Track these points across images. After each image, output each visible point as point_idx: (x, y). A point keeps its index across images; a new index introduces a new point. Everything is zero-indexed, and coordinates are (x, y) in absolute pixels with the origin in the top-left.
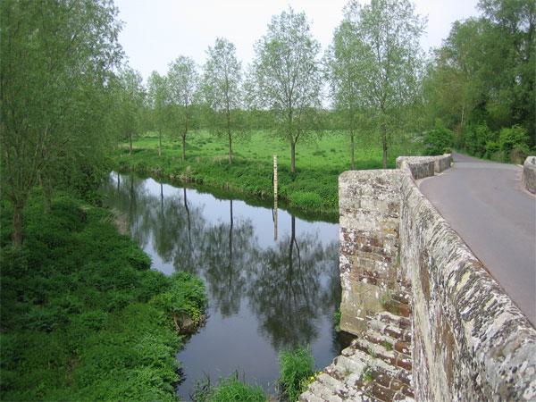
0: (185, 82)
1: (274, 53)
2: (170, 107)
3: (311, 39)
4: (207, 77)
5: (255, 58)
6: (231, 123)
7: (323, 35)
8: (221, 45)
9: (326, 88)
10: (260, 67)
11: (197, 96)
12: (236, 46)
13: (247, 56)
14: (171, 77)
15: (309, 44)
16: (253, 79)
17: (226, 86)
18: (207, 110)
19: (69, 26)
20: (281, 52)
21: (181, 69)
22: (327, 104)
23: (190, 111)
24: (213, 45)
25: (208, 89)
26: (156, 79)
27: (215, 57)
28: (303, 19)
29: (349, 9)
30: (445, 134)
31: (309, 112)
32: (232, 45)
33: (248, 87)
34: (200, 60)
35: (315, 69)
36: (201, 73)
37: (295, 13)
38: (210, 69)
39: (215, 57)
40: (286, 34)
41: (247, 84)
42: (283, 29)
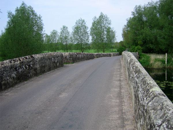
0: (55, 37)
1: (77, 30)
2: (51, 43)
3: (86, 26)
4: (61, 36)
5: (75, 25)
6: (67, 48)
7: (89, 25)
8: (64, 27)
9: (90, 38)
10: (74, 33)
11: (58, 40)
12: (68, 27)
13: (71, 30)
14: (51, 36)
15: (86, 27)
16: (72, 36)
17: (66, 38)
18: (61, 44)
19: (16, 21)
20: (79, 29)
21: (54, 33)
22: (90, 40)
23: (57, 44)
24: (62, 27)
25: (61, 39)
26: (47, 36)
27: (63, 30)
28: (84, 21)
29: (94, 19)
30: (122, 48)
31: (87, 44)
32: (67, 27)
33: (71, 38)
34: (59, 31)
35: (87, 33)
36: (59, 34)
37: (82, 19)
38: (62, 33)
39: (63, 30)
40: (80, 25)
41: (71, 39)
42: (79, 23)
